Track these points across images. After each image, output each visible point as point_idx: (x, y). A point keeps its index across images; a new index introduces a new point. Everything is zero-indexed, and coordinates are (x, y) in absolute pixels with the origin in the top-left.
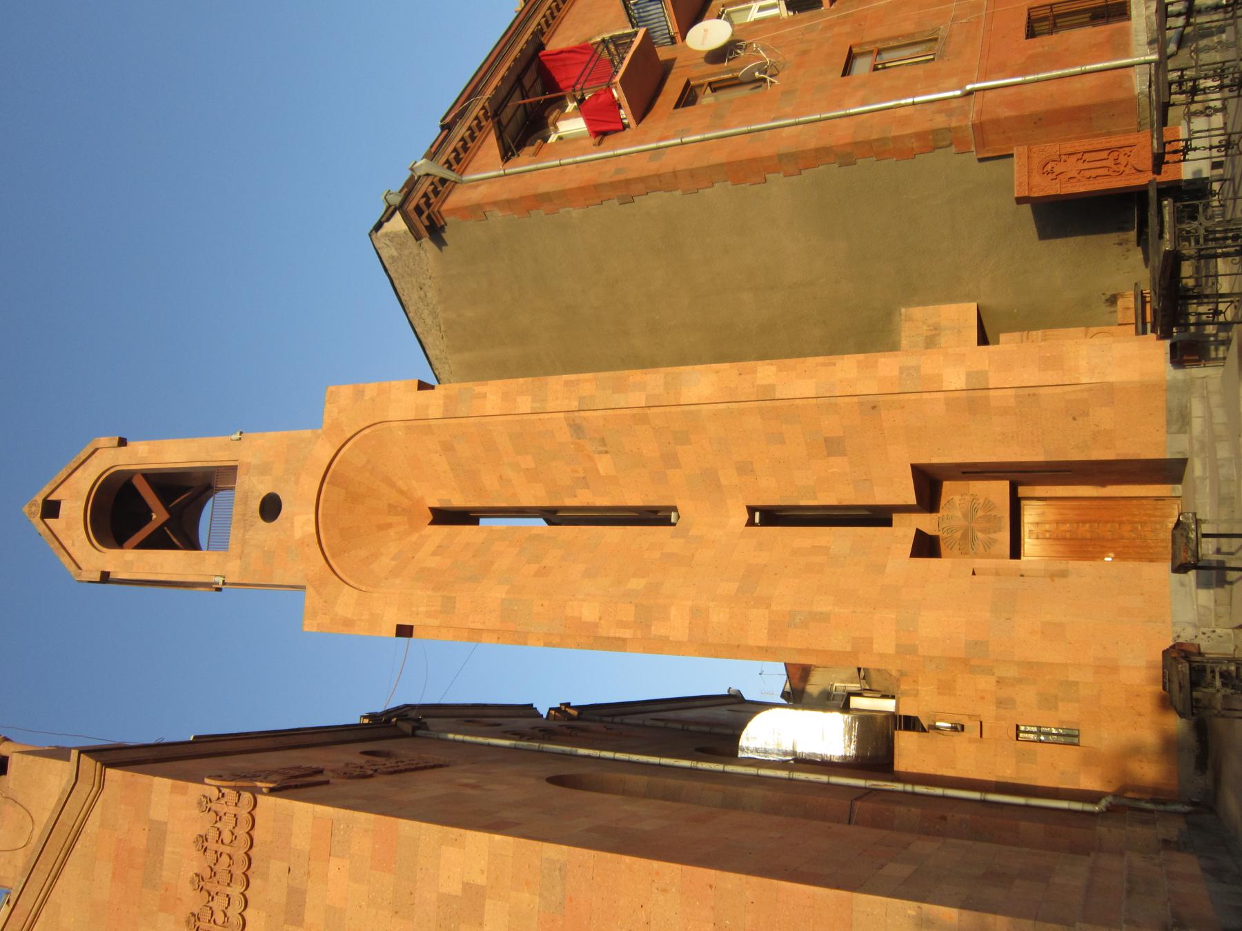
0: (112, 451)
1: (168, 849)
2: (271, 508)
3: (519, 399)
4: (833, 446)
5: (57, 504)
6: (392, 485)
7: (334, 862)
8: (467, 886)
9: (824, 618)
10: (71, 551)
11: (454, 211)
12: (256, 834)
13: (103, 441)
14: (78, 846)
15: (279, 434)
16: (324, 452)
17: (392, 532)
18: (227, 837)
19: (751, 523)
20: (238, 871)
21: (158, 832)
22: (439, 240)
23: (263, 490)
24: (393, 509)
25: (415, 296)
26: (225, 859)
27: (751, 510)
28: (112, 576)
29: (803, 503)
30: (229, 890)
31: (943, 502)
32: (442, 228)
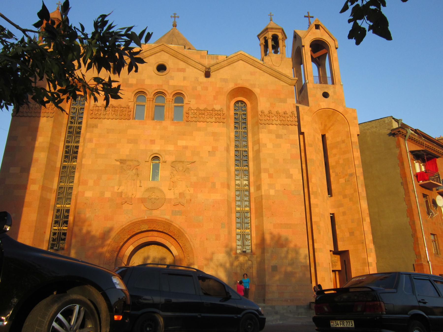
0: (334, 45)
1: (282, 104)
2: (326, 95)
4: (352, 233)
5: (319, 29)
6: (332, 126)
7: (289, 145)
8: (292, 174)
9: (320, 233)
10: (308, 35)
11: (399, 140)
12: (290, 126)
14: (277, 80)
16: (340, 109)
18: (289, 119)
19: (331, 214)
20: (283, 122)
21: (284, 101)
22: (390, 134)
23: (330, 93)
24: (326, 125)
26: (284, 119)
27: (333, 214)
28: (303, 48)
29: (336, 226)
30: (279, 121)
31: (335, 256)
32: (394, 136)
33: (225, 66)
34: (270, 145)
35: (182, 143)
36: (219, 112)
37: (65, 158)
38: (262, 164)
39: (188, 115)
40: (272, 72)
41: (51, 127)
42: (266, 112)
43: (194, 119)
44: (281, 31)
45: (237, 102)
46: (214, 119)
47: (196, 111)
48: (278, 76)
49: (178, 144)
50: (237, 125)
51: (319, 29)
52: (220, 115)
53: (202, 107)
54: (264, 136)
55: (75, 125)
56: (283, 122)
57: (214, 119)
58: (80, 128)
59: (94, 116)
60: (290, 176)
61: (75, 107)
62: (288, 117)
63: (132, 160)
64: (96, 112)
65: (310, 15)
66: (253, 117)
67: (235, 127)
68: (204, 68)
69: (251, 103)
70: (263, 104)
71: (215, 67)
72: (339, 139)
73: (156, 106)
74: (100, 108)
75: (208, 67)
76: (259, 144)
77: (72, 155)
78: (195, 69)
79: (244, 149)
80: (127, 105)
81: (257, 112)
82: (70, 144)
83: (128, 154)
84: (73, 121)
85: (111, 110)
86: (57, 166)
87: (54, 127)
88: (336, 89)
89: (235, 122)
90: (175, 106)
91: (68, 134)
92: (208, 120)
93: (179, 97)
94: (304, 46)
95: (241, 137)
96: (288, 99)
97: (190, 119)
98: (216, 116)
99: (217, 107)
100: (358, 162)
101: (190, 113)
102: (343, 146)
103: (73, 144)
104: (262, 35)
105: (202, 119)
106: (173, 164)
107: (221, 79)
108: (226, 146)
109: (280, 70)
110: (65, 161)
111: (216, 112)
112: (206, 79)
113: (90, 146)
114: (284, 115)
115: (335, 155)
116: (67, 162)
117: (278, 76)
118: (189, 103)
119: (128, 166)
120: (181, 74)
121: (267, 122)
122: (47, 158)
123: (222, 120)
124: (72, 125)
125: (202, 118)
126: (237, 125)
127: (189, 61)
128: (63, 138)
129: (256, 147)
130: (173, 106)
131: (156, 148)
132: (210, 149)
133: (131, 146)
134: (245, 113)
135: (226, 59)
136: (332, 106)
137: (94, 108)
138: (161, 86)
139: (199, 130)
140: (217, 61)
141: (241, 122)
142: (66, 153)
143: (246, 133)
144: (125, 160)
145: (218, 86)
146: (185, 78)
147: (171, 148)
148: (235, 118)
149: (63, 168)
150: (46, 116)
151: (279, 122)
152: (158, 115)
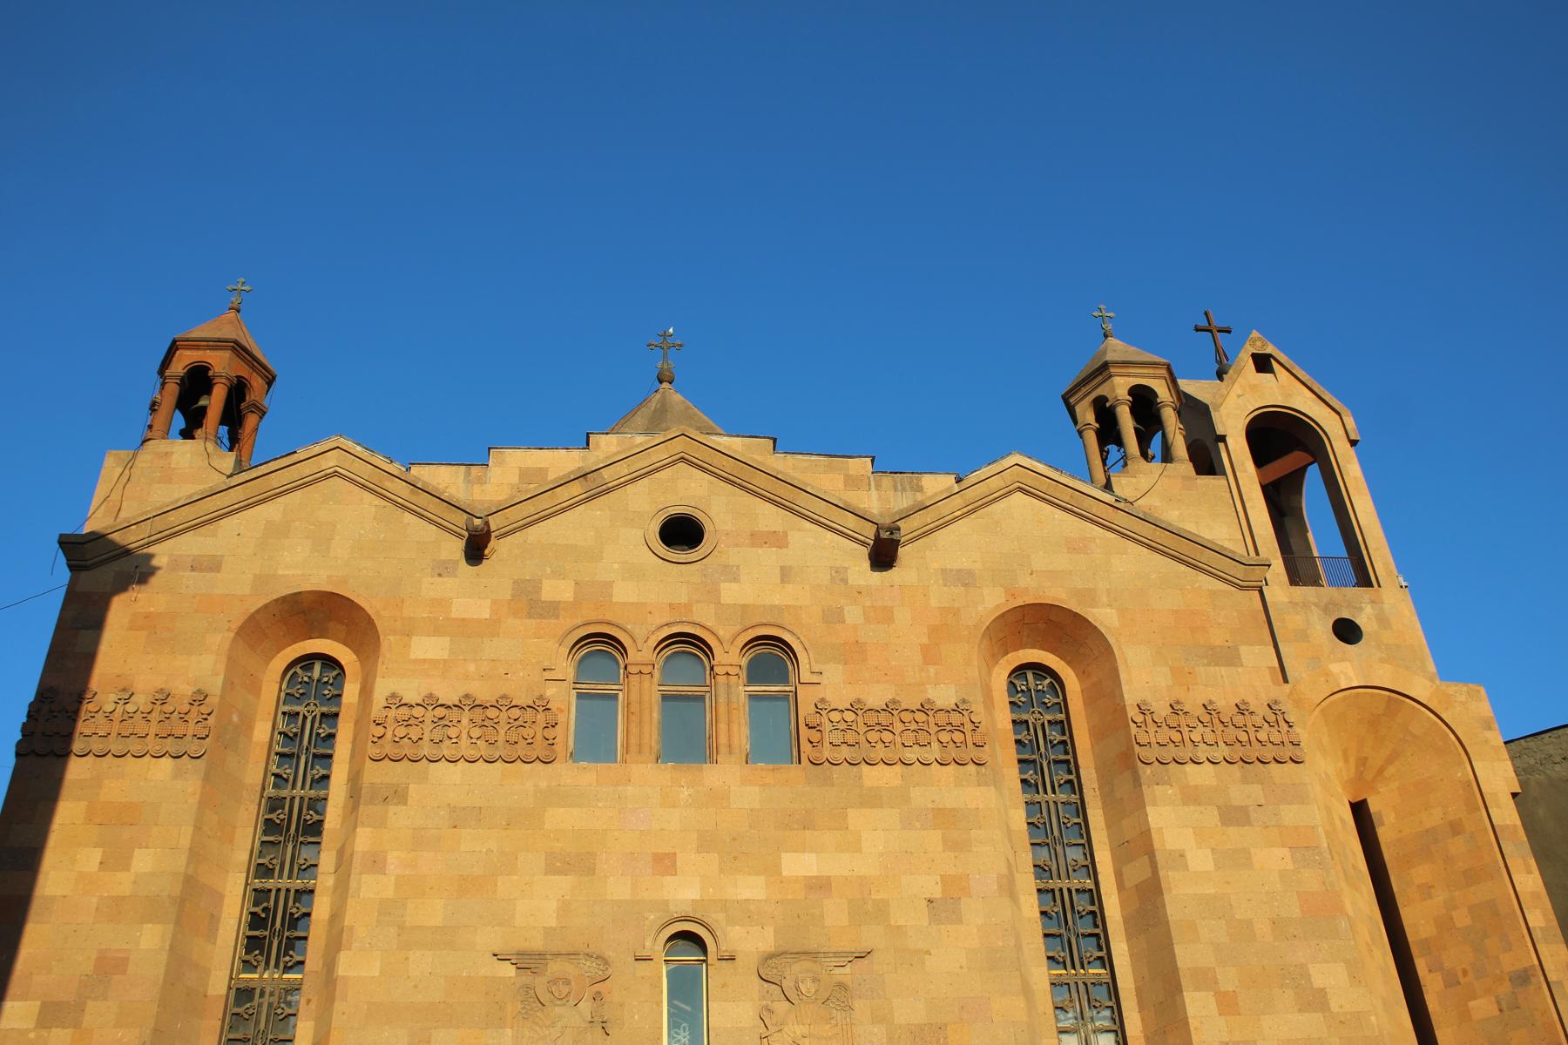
0: (1342, 432)
1: (1223, 670)
2: (1347, 631)
3: (1538, 912)
5: (1270, 370)
6: (1390, 761)
7: (1285, 852)
8: (1322, 991)
12: (1274, 765)
13: (1350, 423)
14: (1183, 567)
15: (1420, 633)
16: (1420, 687)
17: (1341, 764)
20: (1239, 752)
21: (1229, 657)
23: (1360, 621)
24: (1362, 762)
25: (1551, 750)
28: (1221, 445)
30: (1221, 744)
33: (957, 519)
34: (1201, 860)
35: (799, 865)
36: (956, 718)
37: (249, 950)
38: (1178, 950)
39: (815, 736)
40: (1160, 536)
41: (194, 801)
42: (1162, 710)
43: (845, 752)
44: (1163, 372)
45: (1020, 671)
46: (934, 752)
47: (849, 716)
48: (1183, 550)
49: (785, 873)
50: (1030, 775)
51: (1270, 370)
52: (959, 729)
53: (876, 696)
54: (1171, 820)
55: (298, 792)
56: (1239, 752)
57: (934, 752)
58: (318, 804)
59: (389, 749)
60: (1316, 1000)
61: (297, 708)
62: (1258, 728)
63: (572, 955)
64: (401, 731)
65: (1217, 322)
66: (1098, 735)
67: (1024, 781)
68: (869, 532)
69: (1082, 674)
70: (1143, 678)
71: (916, 522)
72: (1434, 818)
73: (665, 698)
74: (418, 712)
75: (887, 521)
76: (1150, 853)
77: (281, 932)
78: (829, 535)
79: (1075, 883)
80: (541, 697)
81: (1123, 710)
82: (271, 883)
83: (553, 923)
84: (288, 771)
85: (465, 721)
86: (211, 992)
87: (204, 803)
88: (1386, 606)
89: (1020, 761)
90: (753, 697)
91: (265, 833)
92: (911, 755)
93: (771, 655)
94: (1223, 439)
95: (1057, 828)
96: (1243, 650)
97: (827, 752)
98: (945, 737)
99: (944, 696)
100: (1541, 916)
101: (827, 726)
102: (1457, 846)
103: (284, 883)
104: (1084, 390)
105: (880, 752)
106: (769, 971)
107: (944, 571)
108: (1004, 871)
109: (1190, 527)
110: (248, 966)
111: (942, 718)
112: (878, 577)
113: (370, 888)
114: (1239, 720)
115: (1427, 891)
116: (253, 969)
117: (1183, 550)
118: (815, 679)
119: (554, 981)
120: (769, 558)
121: (1169, 753)
122: (172, 948)
123: (974, 753)
124: (284, 793)
125: (880, 745)
126: (1030, 775)
127: (803, 500)
128: (242, 856)
129: (1137, 872)
130: (743, 698)
131: (684, 893)
132: (937, 893)
133: (564, 883)
134: (1062, 717)
135: (956, 488)
136: (1384, 676)
137: (392, 713)
138: (688, 607)
139: (872, 799)
140: (919, 497)
141: (1046, 759)
142: (252, 926)
143: (1081, 809)
144: (542, 955)
145: (934, 602)
146: (785, 574)
147: (751, 888)
148: (1018, 742)
149: (238, 1002)
150: (173, 751)
151: (1222, 751)
152: (686, 741)
